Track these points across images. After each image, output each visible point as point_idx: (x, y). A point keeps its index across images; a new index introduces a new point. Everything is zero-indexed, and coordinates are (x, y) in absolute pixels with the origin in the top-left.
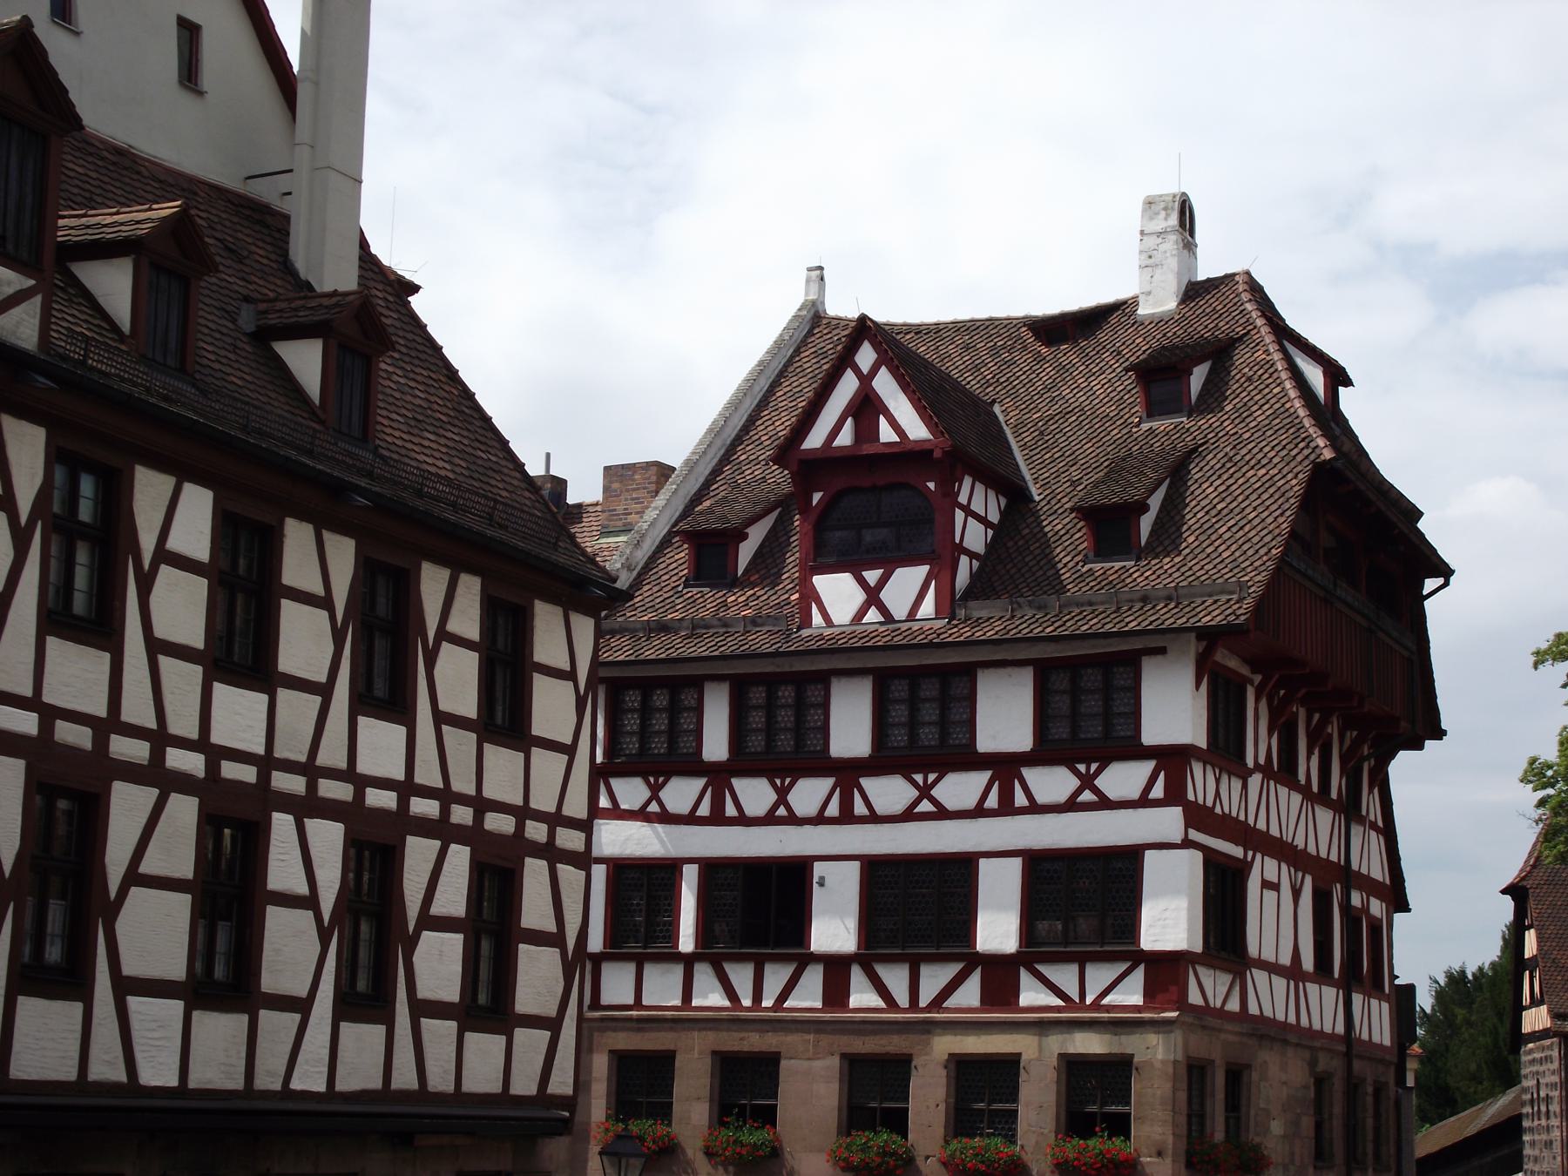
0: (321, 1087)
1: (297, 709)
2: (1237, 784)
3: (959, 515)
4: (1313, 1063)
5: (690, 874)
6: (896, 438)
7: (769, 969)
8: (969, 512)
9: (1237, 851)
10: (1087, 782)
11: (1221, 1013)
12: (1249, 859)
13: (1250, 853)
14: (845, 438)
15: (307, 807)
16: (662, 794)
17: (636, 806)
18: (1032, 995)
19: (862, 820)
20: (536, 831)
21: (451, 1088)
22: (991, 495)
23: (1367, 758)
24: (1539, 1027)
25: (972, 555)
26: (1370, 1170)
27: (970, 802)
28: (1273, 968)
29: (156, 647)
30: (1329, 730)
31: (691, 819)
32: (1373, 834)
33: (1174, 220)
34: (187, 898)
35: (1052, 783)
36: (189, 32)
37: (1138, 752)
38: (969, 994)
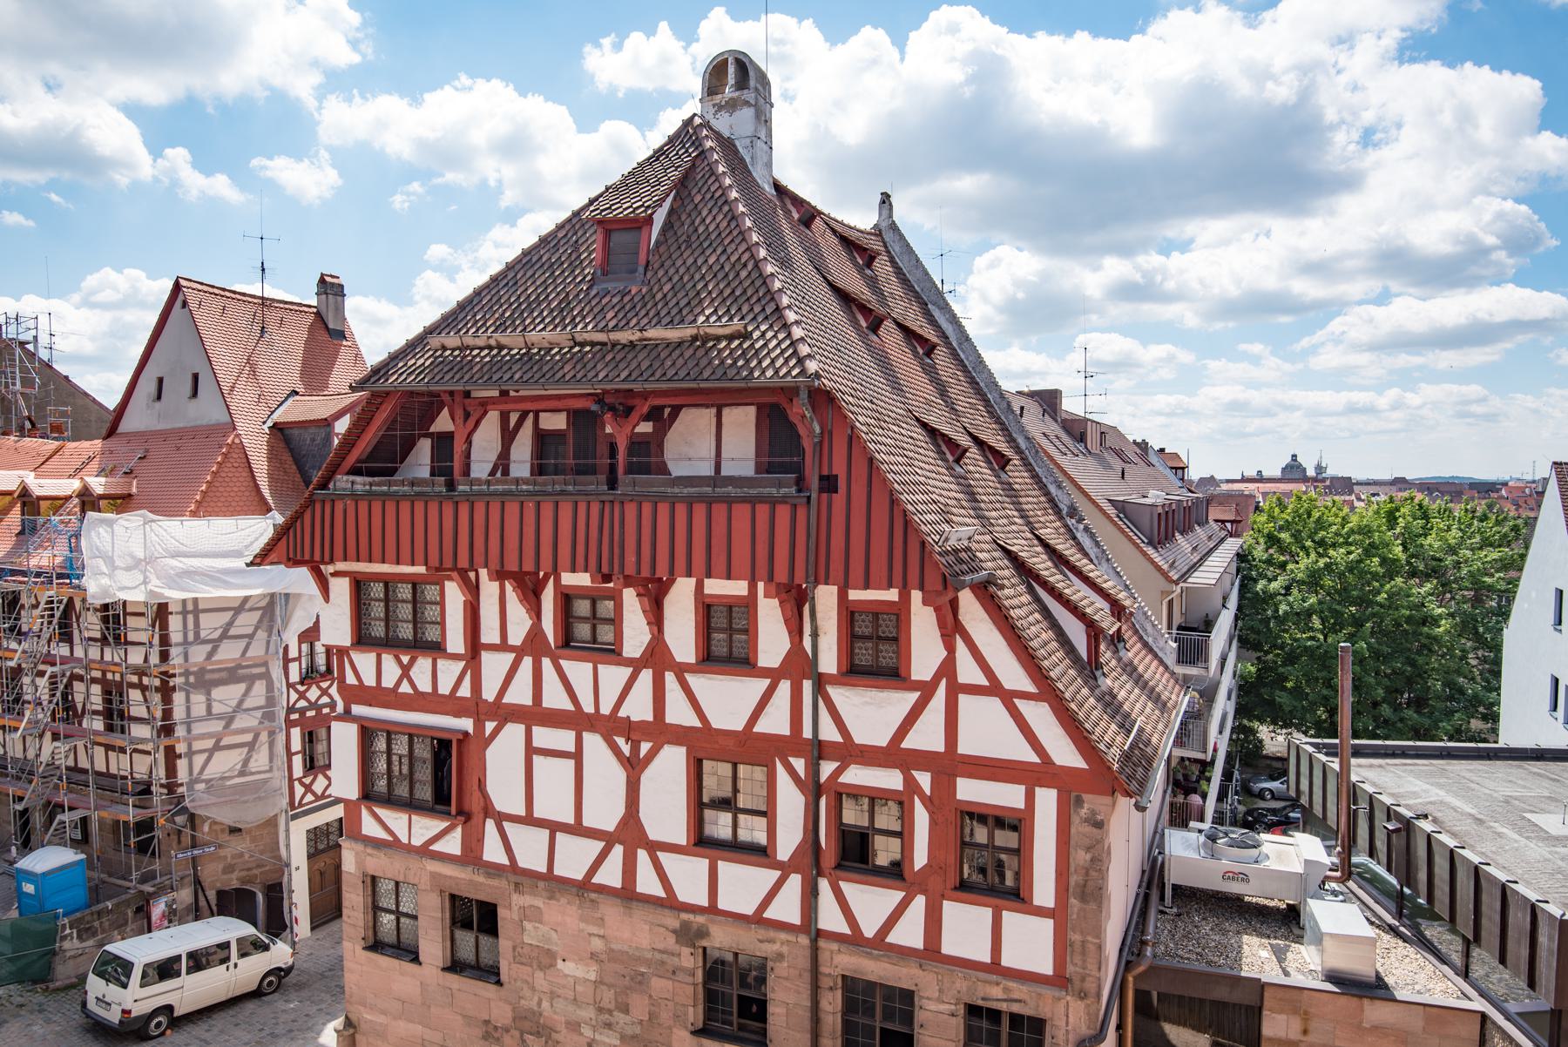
13: (490, 726)
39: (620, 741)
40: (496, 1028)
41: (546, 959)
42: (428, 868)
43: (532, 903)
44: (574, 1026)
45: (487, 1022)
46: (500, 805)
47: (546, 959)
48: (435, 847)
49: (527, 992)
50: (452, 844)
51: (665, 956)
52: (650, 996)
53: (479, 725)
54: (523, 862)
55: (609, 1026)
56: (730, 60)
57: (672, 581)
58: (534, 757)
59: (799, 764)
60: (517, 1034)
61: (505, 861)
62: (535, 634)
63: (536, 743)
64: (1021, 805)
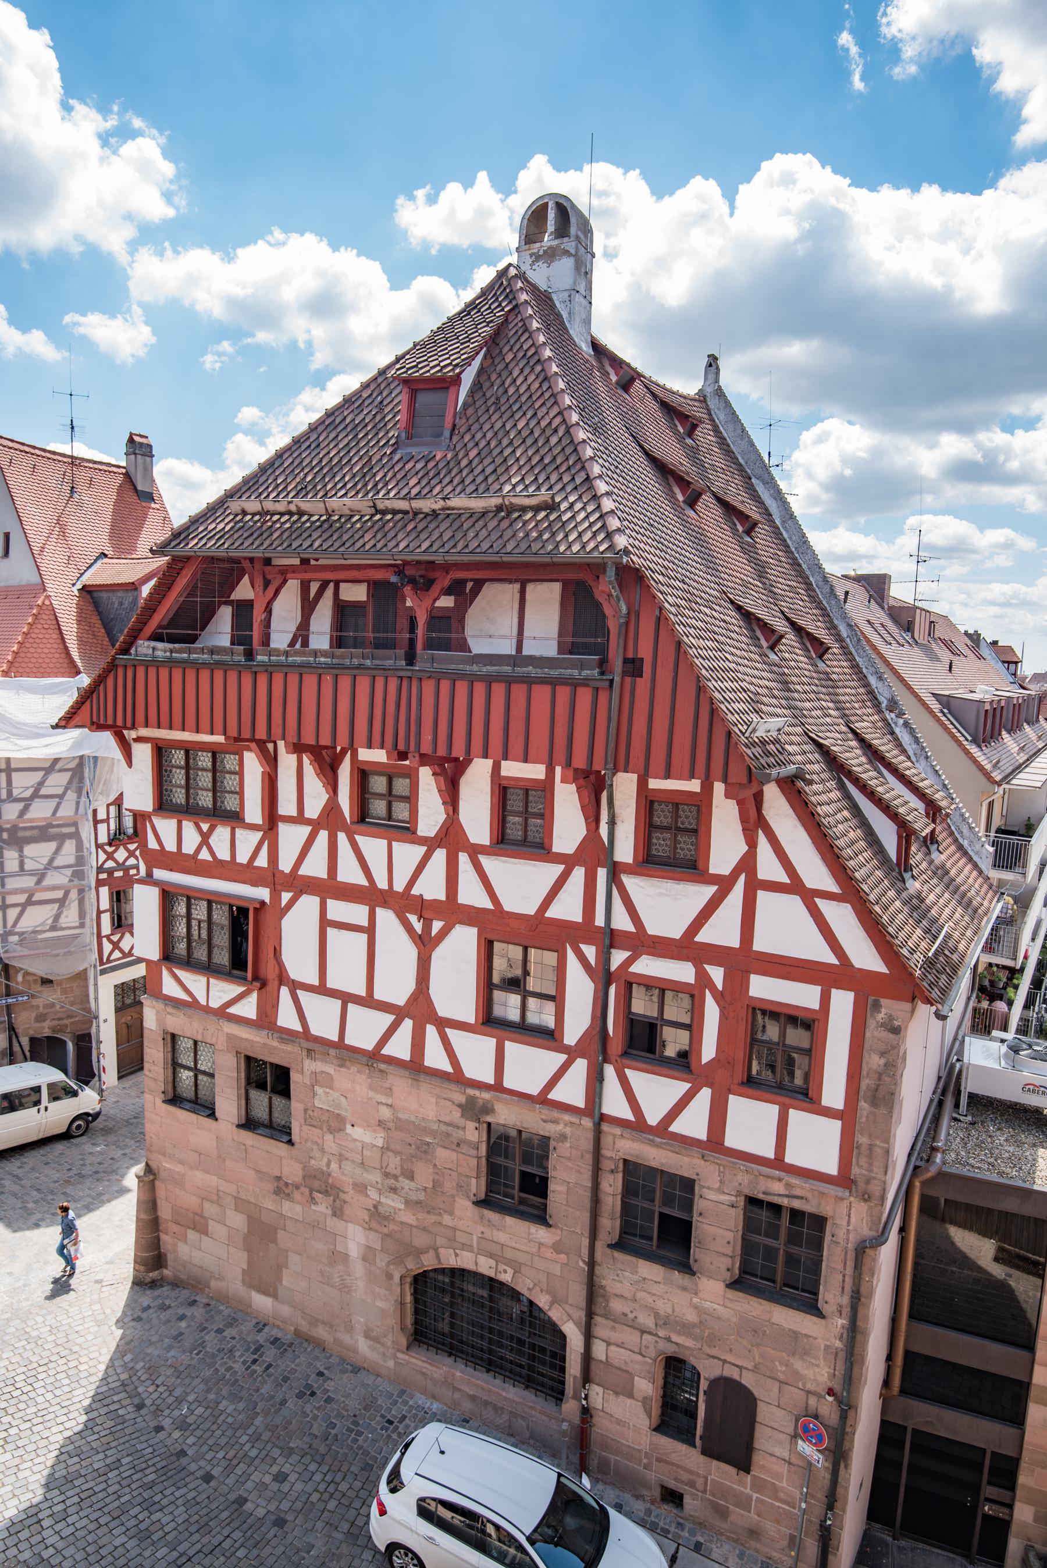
13: (286, 897)
39: (413, 919)
40: (287, 1184)
41: (335, 1123)
42: (225, 1029)
43: (324, 1069)
44: (361, 1188)
45: (278, 1178)
46: (294, 973)
47: (335, 1123)
48: (232, 1010)
49: (316, 1153)
50: (248, 1009)
51: (450, 1129)
52: (435, 1165)
53: (275, 895)
54: (315, 1030)
55: (394, 1190)
56: (551, 205)
57: (468, 761)
58: (328, 929)
59: (590, 952)
60: (307, 1191)
61: (298, 1027)
62: (331, 809)
63: (331, 916)
64: (815, 1005)
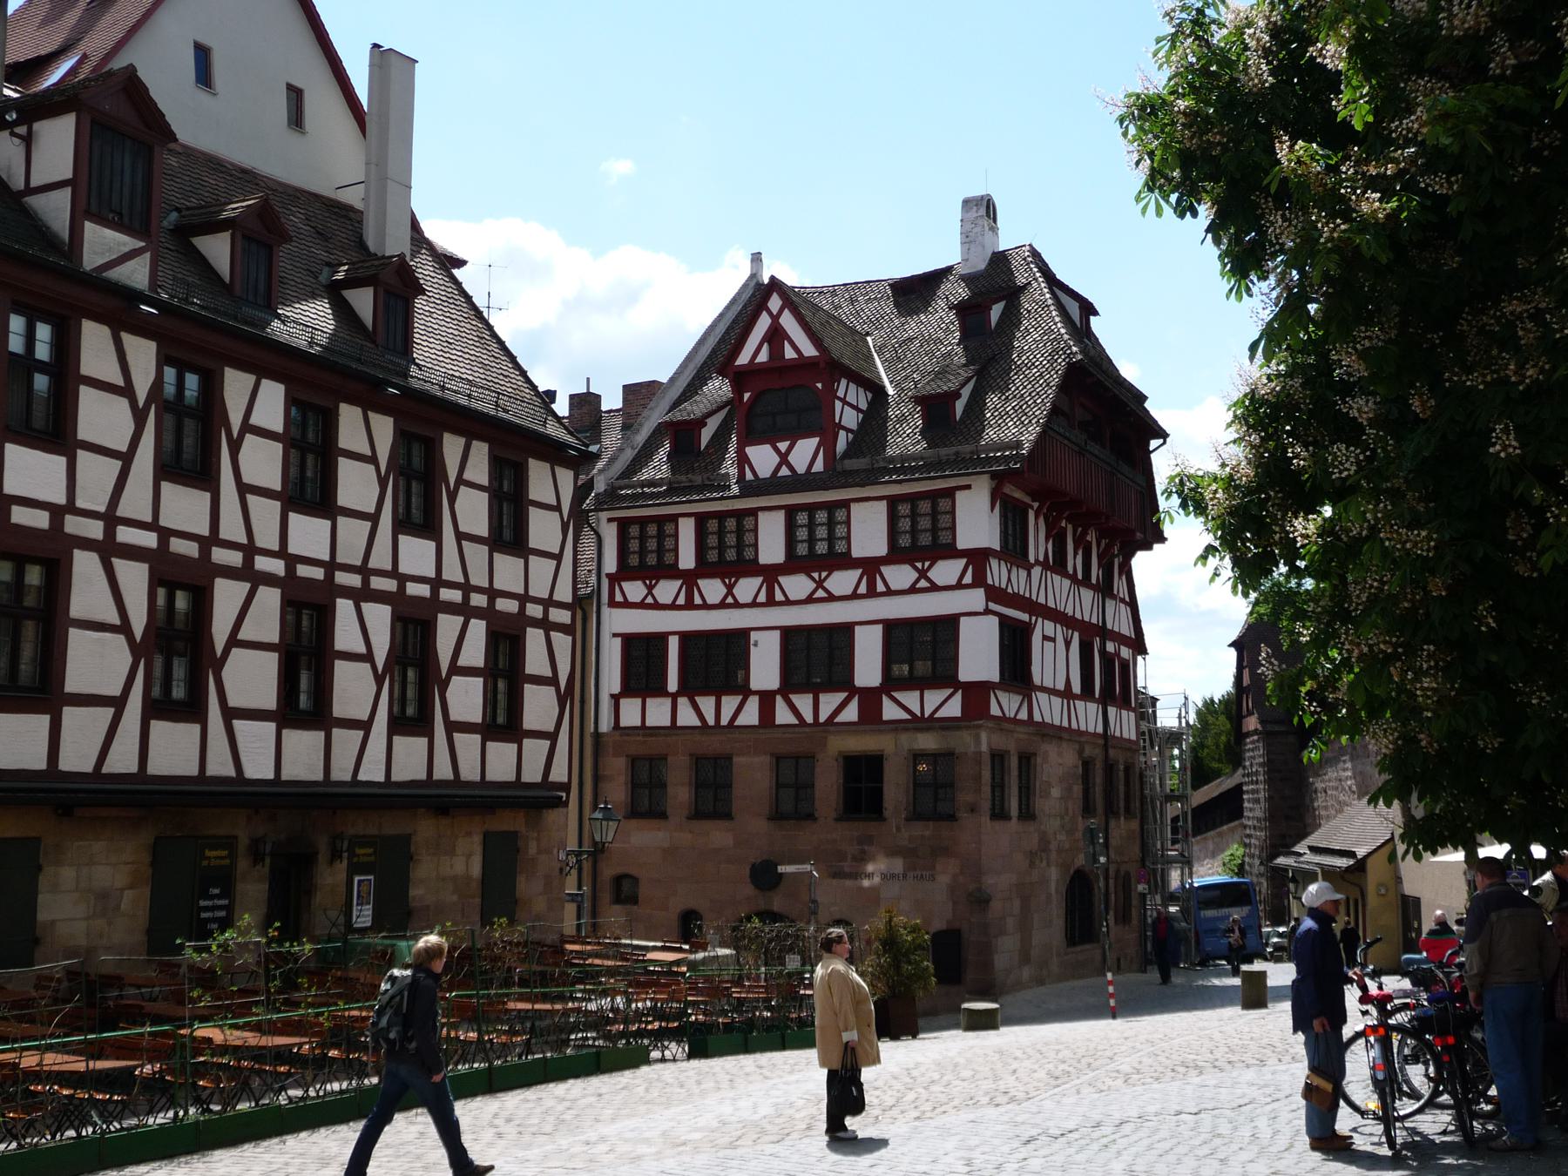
0: (381, 778)
1: (353, 534)
2: (1023, 573)
3: (838, 404)
4: (1081, 752)
5: (674, 644)
6: (795, 356)
7: (724, 699)
8: (844, 402)
9: (1025, 617)
10: (923, 574)
11: (1015, 721)
12: (1033, 621)
13: (1034, 618)
14: (763, 357)
15: (361, 596)
16: (655, 592)
17: (638, 600)
18: (890, 711)
19: (780, 604)
20: (535, 611)
21: (478, 778)
22: (861, 390)
23: (1118, 556)
24: (1252, 728)
25: (848, 430)
26: (1122, 818)
27: (849, 592)
28: (1052, 692)
29: (244, 489)
30: (1089, 538)
31: (673, 606)
32: (1122, 605)
33: (983, 211)
34: (275, 656)
35: (900, 576)
36: (295, 95)
37: (951, 552)
38: (851, 713)
